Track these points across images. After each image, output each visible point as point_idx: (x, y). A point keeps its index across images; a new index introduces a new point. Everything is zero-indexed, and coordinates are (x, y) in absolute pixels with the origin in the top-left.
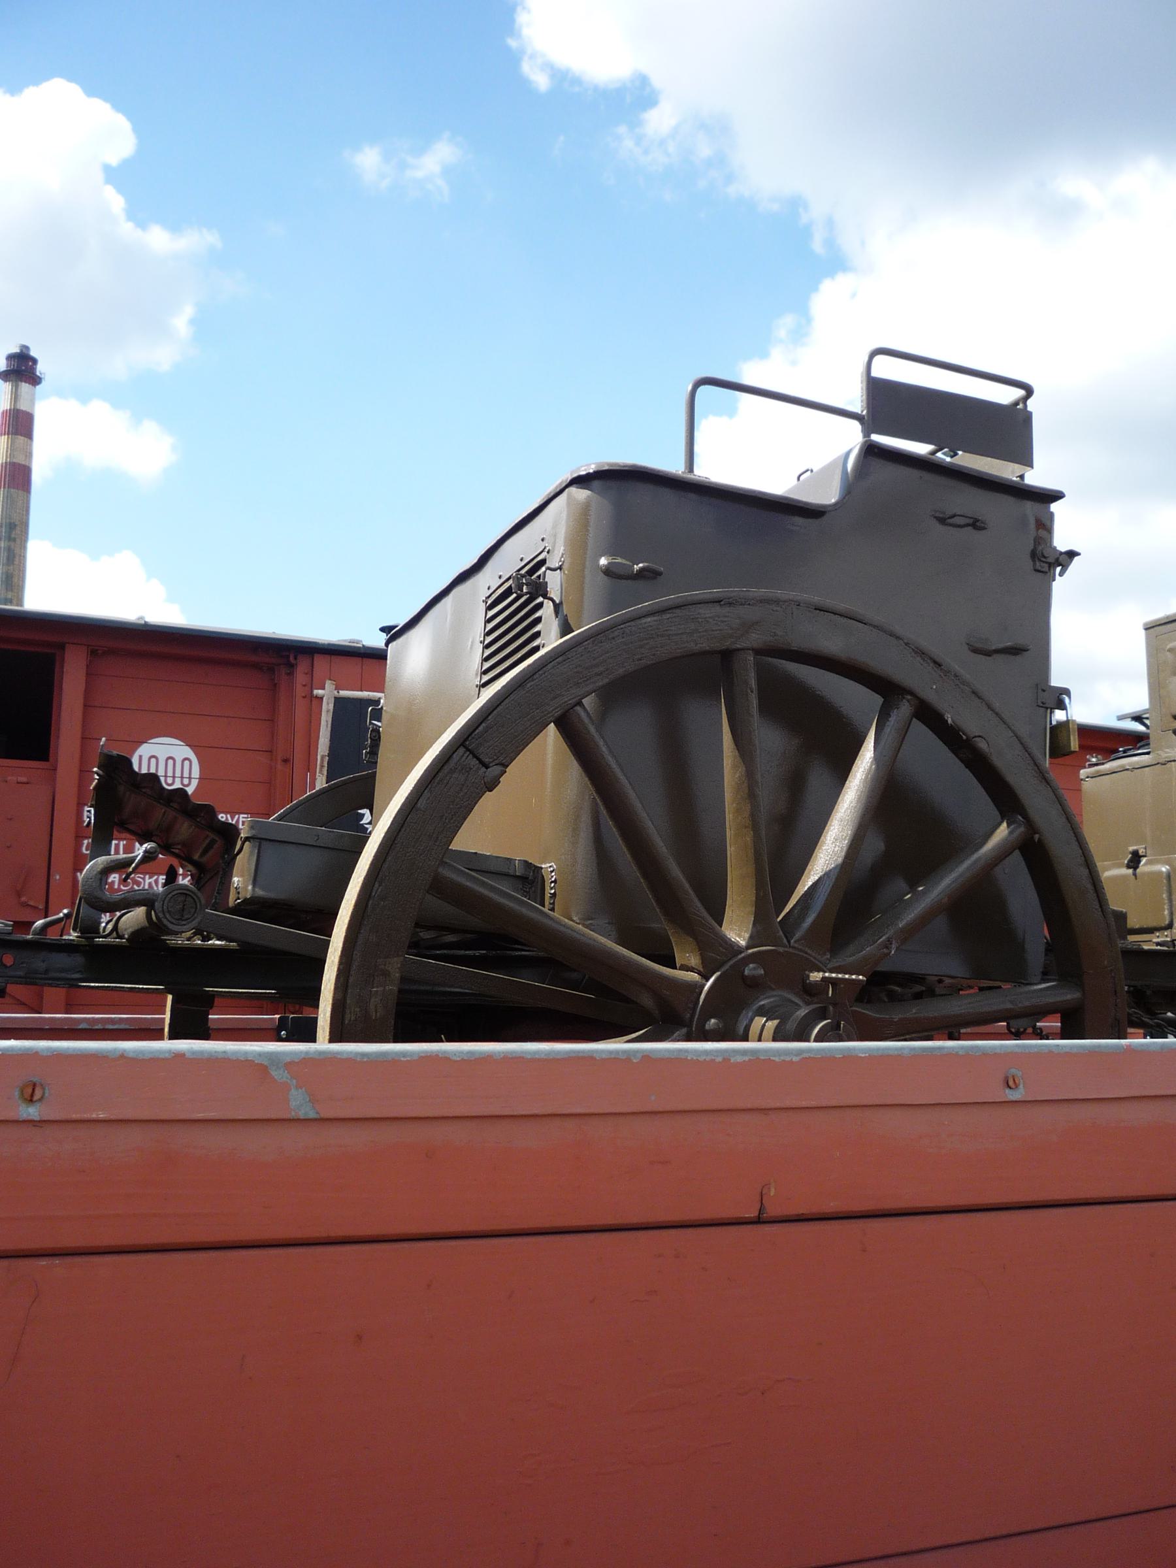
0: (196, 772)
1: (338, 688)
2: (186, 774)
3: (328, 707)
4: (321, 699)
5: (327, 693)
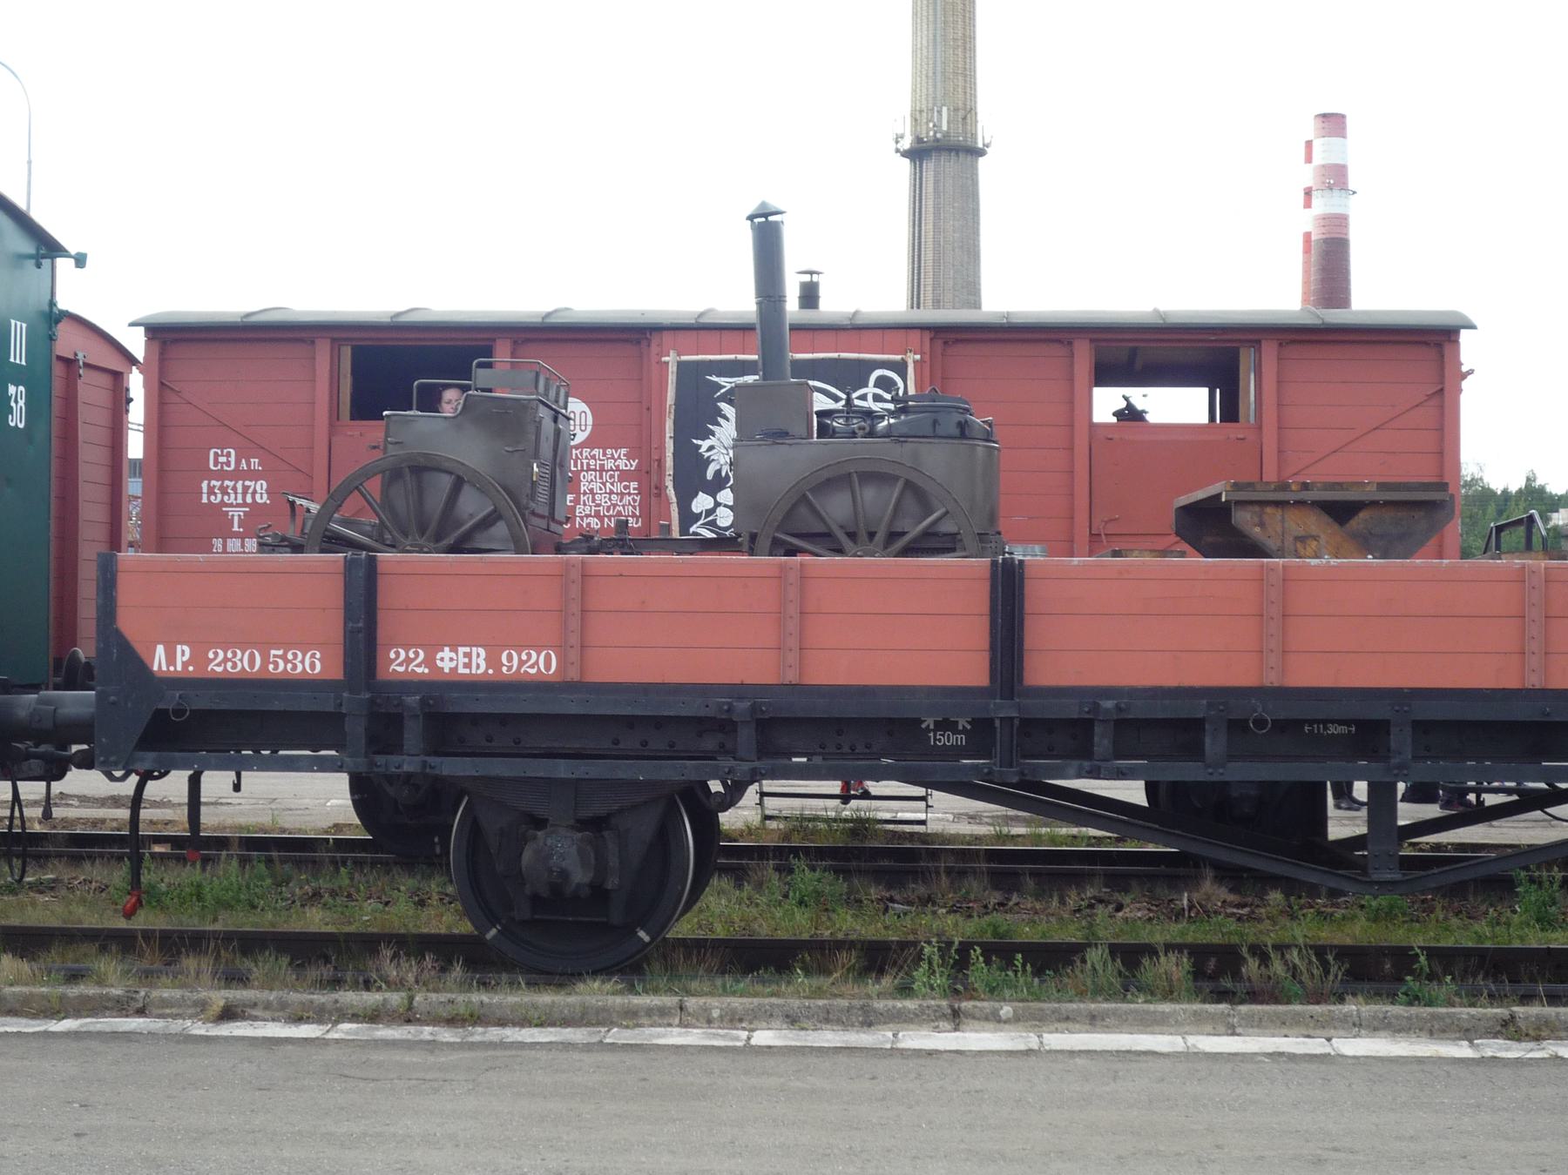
0: (590, 421)
1: (679, 355)
2: (583, 423)
3: (673, 369)
4: (667, 363)
5: (671, 359)
